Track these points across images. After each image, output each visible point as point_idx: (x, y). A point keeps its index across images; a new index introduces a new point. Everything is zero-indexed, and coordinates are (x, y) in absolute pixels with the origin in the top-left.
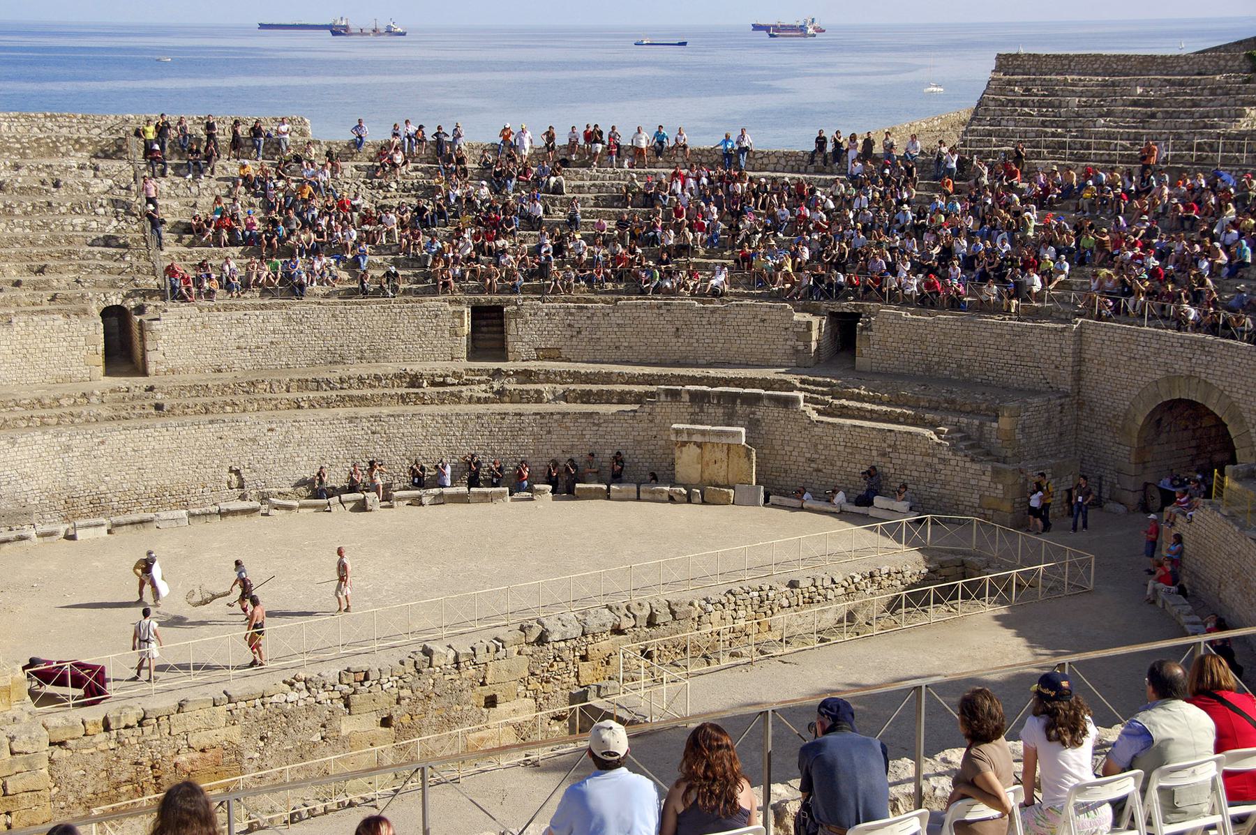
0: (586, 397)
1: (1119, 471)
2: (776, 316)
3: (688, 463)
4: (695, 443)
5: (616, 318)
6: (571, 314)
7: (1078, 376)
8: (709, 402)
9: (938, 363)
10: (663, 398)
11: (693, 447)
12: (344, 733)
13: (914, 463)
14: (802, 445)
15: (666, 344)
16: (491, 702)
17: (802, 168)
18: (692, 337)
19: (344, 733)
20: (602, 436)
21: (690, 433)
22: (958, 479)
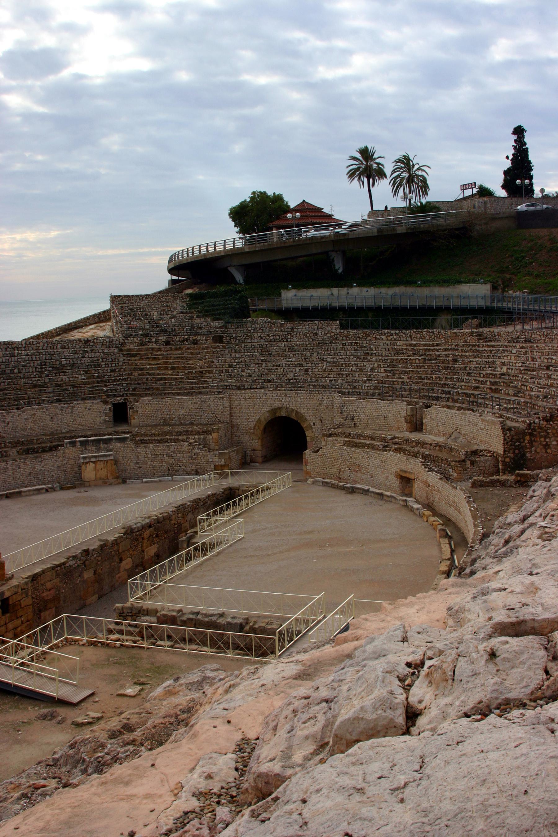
0: (27, 452)
1: (254, 450)
2: (95, 407)
3: (89, 472)
4: (92, 462)
5: (24, 416)
6: (4, 416)
7: (231, 416)
8: (89, 444)
9: (169, 418)
10: (68, 445)
11: (91, 464)
12: (85, 578)
13: (183, 457)
14: (132, 457)
15: (47, 425)
16: (121, 560)
17: (55, 347)
18: (58, 420)
19: (85, 578)
20: (43, 467)
21: (90, 458)
22: (203, 460)
